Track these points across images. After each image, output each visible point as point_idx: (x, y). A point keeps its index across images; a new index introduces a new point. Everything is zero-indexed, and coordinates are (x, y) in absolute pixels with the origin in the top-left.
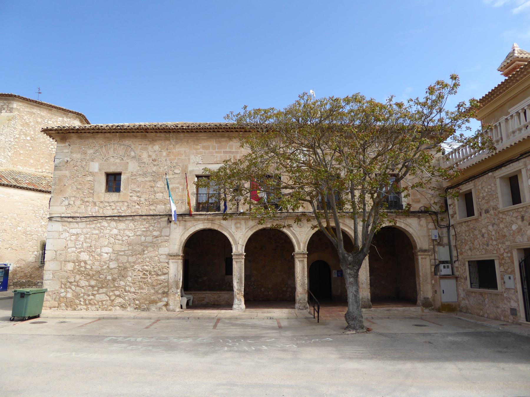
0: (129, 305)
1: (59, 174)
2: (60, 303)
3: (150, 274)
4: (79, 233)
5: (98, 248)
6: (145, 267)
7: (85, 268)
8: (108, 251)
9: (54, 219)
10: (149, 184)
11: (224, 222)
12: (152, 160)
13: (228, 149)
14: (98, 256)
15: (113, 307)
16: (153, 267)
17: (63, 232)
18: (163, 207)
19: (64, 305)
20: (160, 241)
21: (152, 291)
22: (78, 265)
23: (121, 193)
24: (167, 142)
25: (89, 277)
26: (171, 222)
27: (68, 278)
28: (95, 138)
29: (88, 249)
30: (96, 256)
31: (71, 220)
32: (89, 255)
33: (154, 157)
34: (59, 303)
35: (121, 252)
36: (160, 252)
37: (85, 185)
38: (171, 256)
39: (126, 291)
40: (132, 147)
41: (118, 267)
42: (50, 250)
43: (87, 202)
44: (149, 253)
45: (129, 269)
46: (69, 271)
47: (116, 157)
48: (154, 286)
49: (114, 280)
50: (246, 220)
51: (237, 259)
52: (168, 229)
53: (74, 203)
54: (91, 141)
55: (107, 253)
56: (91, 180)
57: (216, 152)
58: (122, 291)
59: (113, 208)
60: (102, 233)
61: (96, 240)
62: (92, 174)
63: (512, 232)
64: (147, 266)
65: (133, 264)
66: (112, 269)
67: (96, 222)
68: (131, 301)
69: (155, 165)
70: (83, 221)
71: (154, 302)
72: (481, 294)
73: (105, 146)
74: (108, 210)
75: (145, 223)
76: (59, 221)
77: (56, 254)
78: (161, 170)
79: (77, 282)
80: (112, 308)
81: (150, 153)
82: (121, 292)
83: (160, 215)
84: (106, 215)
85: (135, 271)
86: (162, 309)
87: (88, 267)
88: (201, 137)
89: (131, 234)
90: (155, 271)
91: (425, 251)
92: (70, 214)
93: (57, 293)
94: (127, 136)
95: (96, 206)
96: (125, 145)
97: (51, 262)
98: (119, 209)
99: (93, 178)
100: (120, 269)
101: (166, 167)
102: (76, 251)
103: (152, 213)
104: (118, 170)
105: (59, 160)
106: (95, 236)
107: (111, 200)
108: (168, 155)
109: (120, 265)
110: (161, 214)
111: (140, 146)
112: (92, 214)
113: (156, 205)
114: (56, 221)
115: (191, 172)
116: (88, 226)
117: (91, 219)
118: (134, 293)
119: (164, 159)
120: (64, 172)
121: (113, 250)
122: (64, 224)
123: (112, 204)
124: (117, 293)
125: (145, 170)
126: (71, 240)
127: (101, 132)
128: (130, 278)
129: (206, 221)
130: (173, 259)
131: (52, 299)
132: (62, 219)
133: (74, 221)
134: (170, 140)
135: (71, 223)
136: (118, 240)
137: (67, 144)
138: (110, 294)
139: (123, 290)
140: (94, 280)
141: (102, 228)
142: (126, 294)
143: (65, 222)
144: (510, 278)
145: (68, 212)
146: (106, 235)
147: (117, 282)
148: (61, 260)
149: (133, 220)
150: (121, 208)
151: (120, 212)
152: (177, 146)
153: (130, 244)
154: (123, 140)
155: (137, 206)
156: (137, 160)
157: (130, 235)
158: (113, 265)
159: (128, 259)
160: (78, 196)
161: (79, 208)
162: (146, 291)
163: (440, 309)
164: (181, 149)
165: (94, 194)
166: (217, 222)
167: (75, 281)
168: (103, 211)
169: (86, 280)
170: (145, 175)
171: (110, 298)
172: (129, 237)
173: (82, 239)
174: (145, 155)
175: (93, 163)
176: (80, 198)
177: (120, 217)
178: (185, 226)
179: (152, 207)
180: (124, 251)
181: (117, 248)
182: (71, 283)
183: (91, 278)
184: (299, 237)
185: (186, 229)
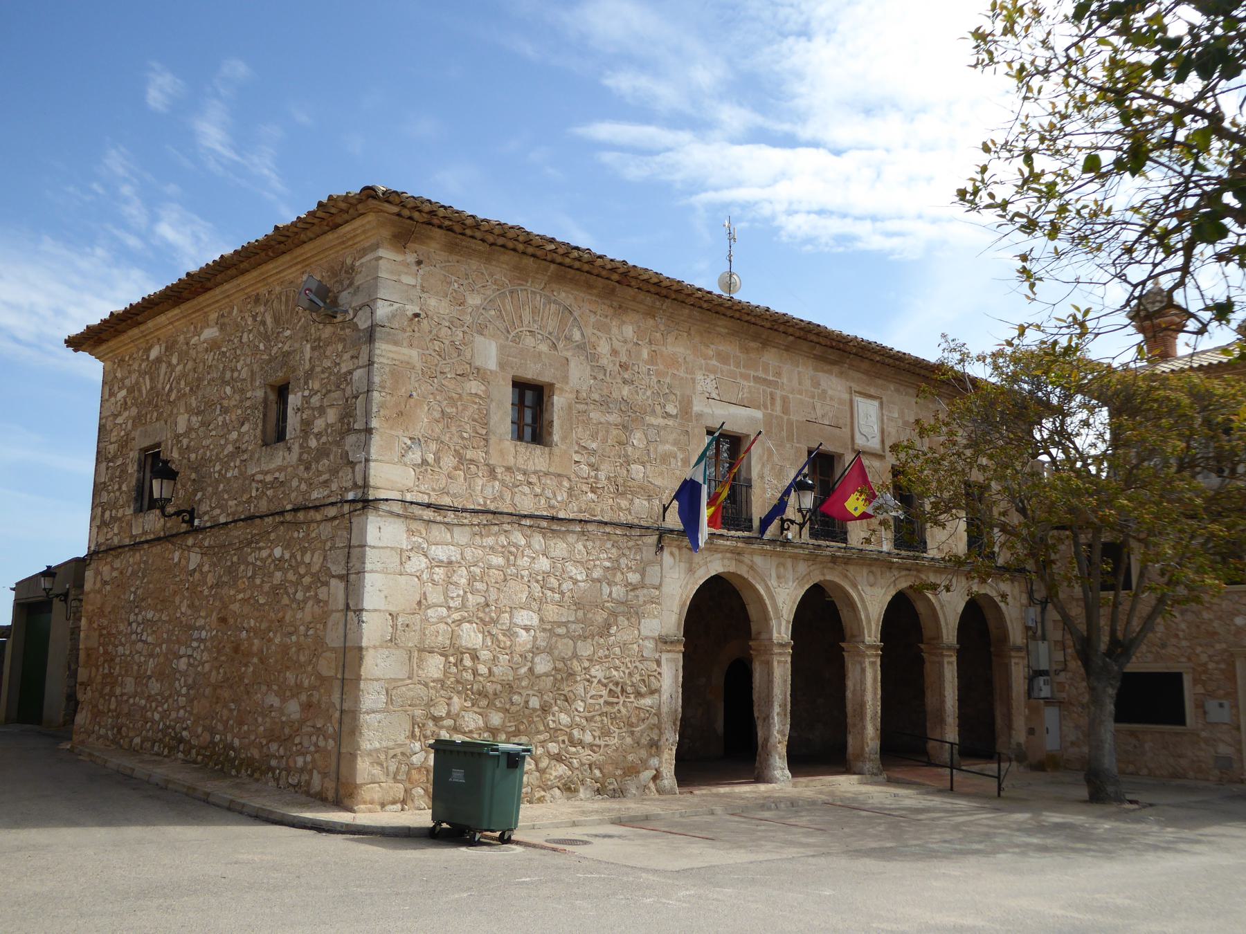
0: (583, 782)
1: (391, 355)
2: (411, 786)
3: (623, 690)
4: (453, 559)
5: (506, 612)
6: (615, 673)
7: (475, 673)
8: (529, 623)
9: (384, 507)
10: (615, 432)
11: (758, 560)
12: (621, 366)
13: (761, 374)
14: (504, 635)
15: (544, 790)
16: (630, 673)
17: (411, 555)
18: (646, 503)
19: (422, 792)
20: (641, 599)
21: (629, 740)
22: (455, 665)
23: (556, 450)
24: (651, 322)
25: (484, 703)
26: (662, 549)
27: (430, 703)
28: (488, 260)
29: (481, 615)
30: (501, 637)
31: (428, 514)
32: (483, 633)
33: (624, 359)
34: (409, 786)
35: (559, 627)
36: (644, 632)
37: (465, 408)
38: (663, 641)
39: (572, 743)
40: (576, 314)
41: (553, 673)
42: (375, 610)
43: (472, 461)
44: (622, 633)
45: (579, 678)
46: (433, 681)
47: (540, 337)
48: (631, 725)
49: (545, 709)
50: (795, 557)
51: (780, 654)
52: (657, 568)
53: (437, 460)
54: (474, 264)
55: (527, 629)
56: (480, 393)
57: (742, 375)
58: (563, 741)
59: (538, 491)
60: (514, 565)
61: (497, 586)
62: (480, 374)
63: (1233, 628)
64: (616, 668)
65: (586, 664)
66: (538, 677)
67: (496, 528)
68: (585, 771)
69: (625, 382)
70: (466, 521)
71: (632, 771)
72: (1133, 734)
73: (511, 292)
74: (525, 494)
75: (610, 546)
76: (398, 515)
77: (394, 626)
78: (640, 398)
79: (455, 718)
80: (543, 793)
81: (617, 345)
82: (562, 746)
83: (641, 527)
84: (522, 512)
85: (592, 682)
86: (649, 788)
87: (483, 669)
88: (718, 328)
89: (578, 573)
90: (633, 685)
91: (1019, 649)
92: (428, 494)
93: (400, 757)
94: (572, 280)
95: (495, 478)
96: (559, 304)
97: (381, 650)
98: (551, 495)
99: (483, 388)
100: (559, 677)
101: (649, 393)
102: (449, 616)
103: (623, 518)
104: (545, 378)
105: (391, 308)
106: (496, 572)
107: (531, 468)
108: (652, 360)
109: (560, 665)
110: (643, 523)
111: (592, 316)
112: (485, 503)
113: (630, 497)
114: (391, 513)
115: (700, 416)
116: (478, 539)
117: (483, 518)
118: (591, 746)
119: (644, 369)
120: (406, 351)
121: (541, 620)
122: (415, 525)
123: (534, 479)
124: (553, 748)
125: (605, 392)
126: (434, 582)
127: (514, 250)
128: (582, 704)
129: (728, 555)
130: (669, 651)
131: (388, 775)
132: (405, 509)
133: (439, 519)
134: (654, 316)
135: (434, 526)
136: (550, 589)
137: (411, 258)
138: (538, 752)
139: (566, 738)
140: (498, 710)
141: (513, 549)
142: (573, 749)
143: (414, 518)
144: (1221, 705)
145: (423, 489)
146: (523, 572)
147: (554, 716)
148: (410, 644)
149: (583, 533)
150: (555, 495)
151: (553, 507)
152: (670, 339)
153: (578, 605)
154: (554, 286)
155: (590, 495)
156: (587, 357)
157: (579, 578)
158: (543, 665)
159: (575, 648)
160: (446, 439)
161: (450, 478)
162: (615, 741)
163: (1040, 767)
164: (678, 350)
165: (491, 442)
166: (747, 559)
167: (448, 714)
168: (512, 499)
169: (478, 710)
170: (605, 404)
171: (537, 765)
172: (576, 582)
173: (463, 581)
174: (604, 348)
175: (482, 338)
176: (452, 448)
177: (552, 523)
178: (690, 562)
179: (624, 503)
180: (565, 624)
181: (552, 612)
182: (436, 720)
183: (491, 705)
184: (870, 609)
185: (691, 570)
